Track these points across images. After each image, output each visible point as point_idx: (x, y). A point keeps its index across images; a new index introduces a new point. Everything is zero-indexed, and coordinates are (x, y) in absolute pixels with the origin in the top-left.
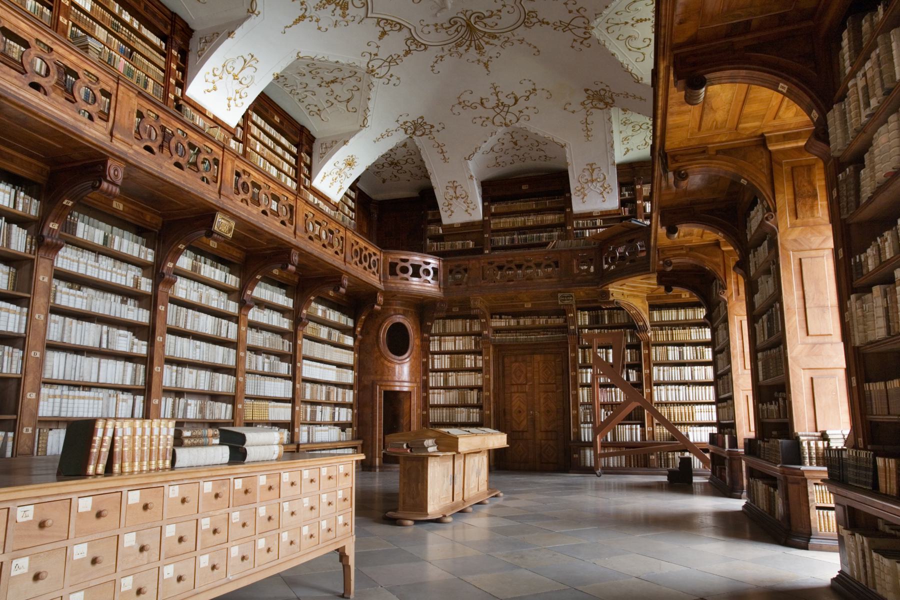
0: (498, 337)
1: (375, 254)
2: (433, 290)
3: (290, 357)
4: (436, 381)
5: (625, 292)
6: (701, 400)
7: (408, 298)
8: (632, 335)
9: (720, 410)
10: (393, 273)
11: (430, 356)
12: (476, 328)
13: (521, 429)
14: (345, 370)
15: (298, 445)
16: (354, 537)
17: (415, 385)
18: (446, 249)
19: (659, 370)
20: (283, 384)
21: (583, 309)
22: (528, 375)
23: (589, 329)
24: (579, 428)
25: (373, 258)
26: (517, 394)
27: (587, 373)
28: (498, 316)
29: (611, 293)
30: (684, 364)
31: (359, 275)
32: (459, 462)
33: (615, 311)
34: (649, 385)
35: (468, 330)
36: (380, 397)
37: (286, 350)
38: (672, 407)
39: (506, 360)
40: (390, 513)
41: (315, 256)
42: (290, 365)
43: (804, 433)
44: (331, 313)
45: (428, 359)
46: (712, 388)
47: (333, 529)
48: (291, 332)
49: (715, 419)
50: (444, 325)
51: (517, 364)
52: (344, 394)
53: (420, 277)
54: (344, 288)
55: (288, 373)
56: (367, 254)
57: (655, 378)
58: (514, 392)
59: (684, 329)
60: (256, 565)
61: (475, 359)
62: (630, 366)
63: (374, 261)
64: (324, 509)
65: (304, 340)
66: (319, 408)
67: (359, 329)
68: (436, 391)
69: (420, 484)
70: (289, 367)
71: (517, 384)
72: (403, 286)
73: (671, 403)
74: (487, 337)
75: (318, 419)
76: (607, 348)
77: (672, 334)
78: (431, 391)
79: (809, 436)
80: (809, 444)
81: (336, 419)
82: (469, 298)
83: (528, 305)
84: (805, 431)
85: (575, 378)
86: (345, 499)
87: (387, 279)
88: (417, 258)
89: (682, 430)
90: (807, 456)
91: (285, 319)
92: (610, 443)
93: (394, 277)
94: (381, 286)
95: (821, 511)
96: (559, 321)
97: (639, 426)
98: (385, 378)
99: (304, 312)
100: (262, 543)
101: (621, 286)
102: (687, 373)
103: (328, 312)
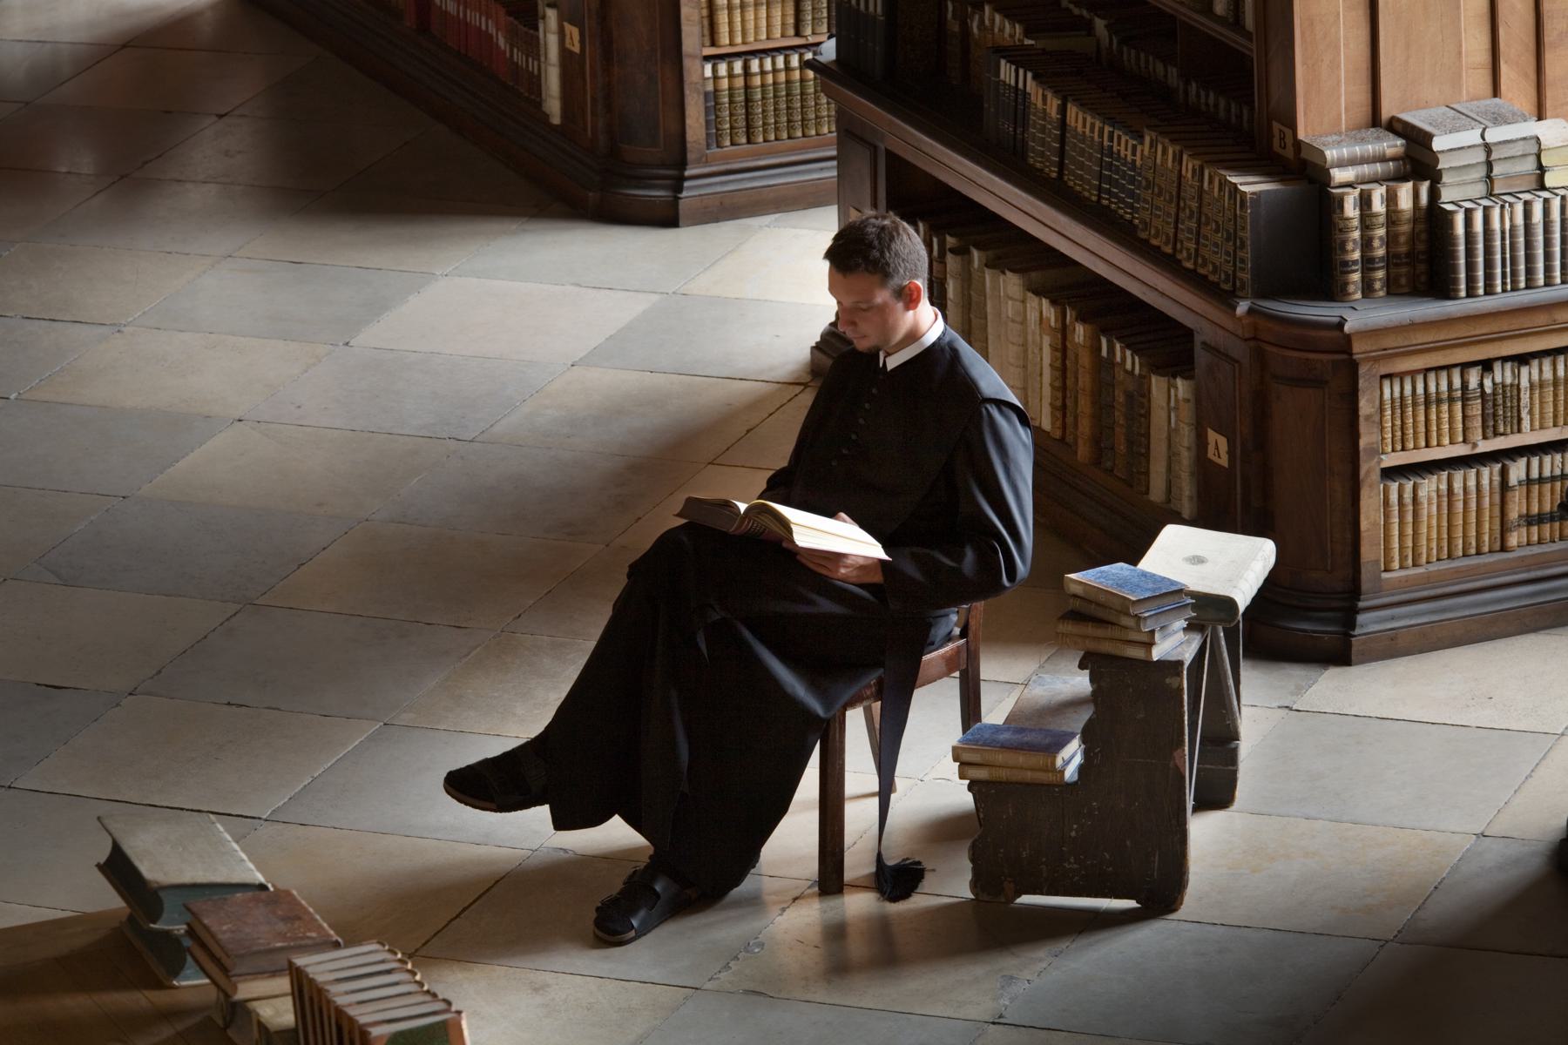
80: (1365, 201)
95: (1394, 486)
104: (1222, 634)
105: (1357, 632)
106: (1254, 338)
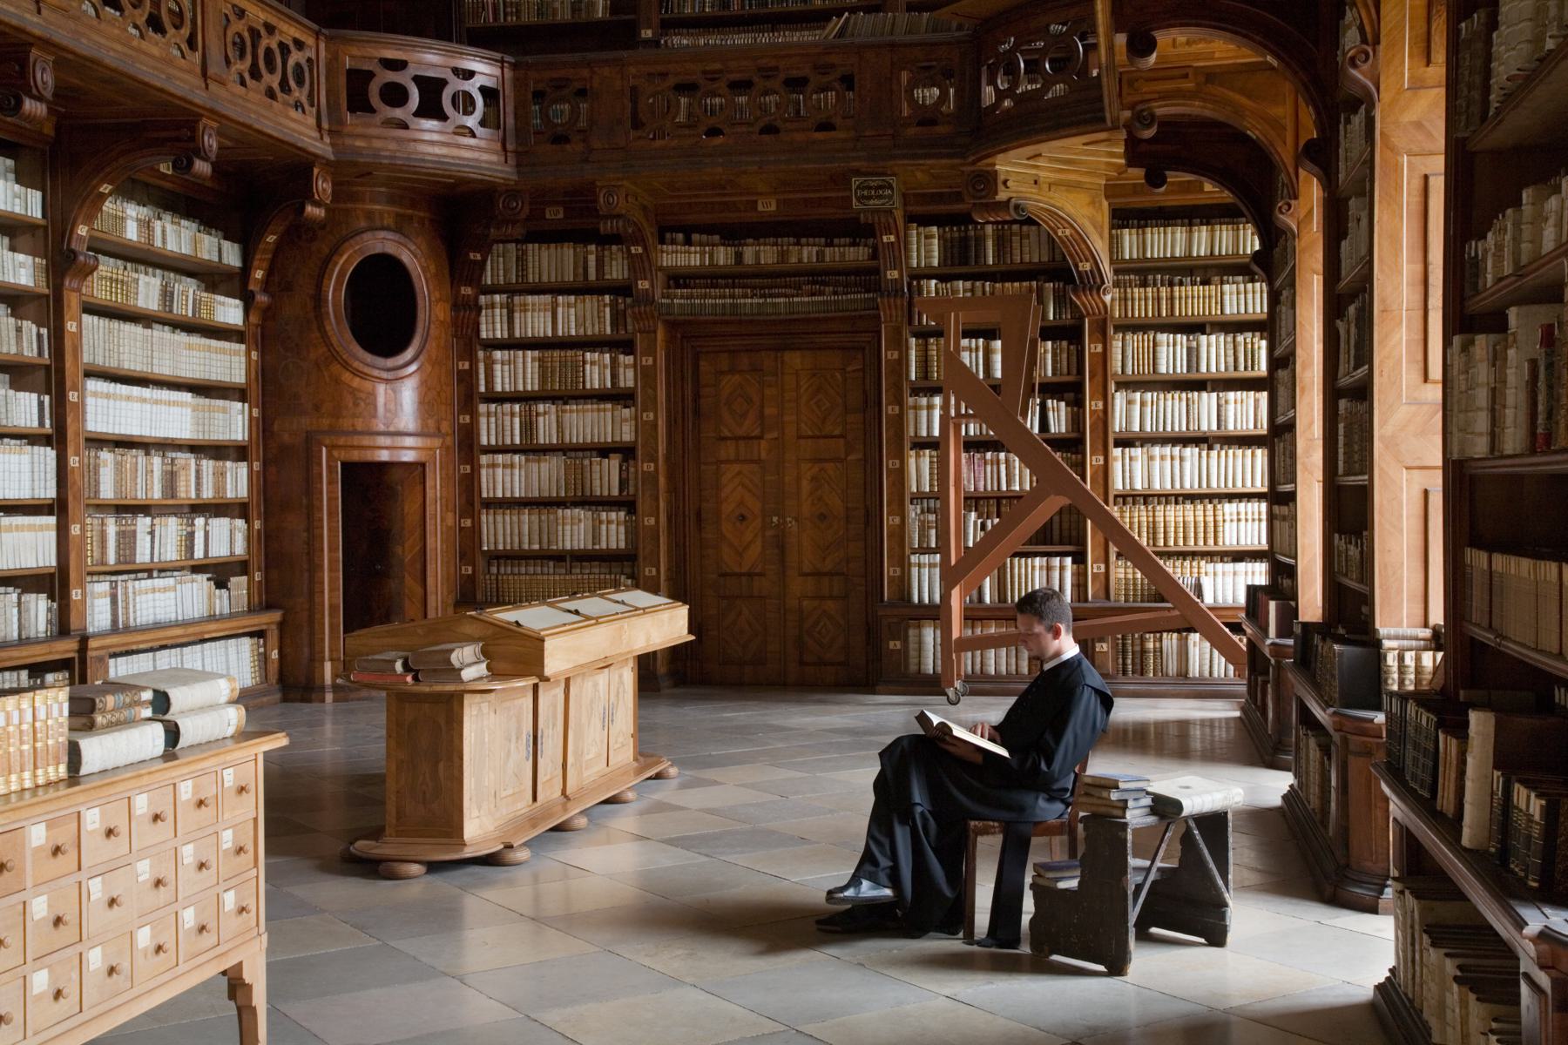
0: (680, 300)
1: (299, 45)
2: (485, 157)
3: (41, 374)
4: (500, 430)
5: (1042, 174)
6: (1239, 489)
7: (406, 180)
8: (1061, 300)
9: (1277, 523)
10: (359, 103)
11: (481, 354)
12: (617, 271)
13: (745, 570)
14: (220, 403)
15: (84, 640)
16: (265, 937)
17: (437, 442)
18: (525, 19)
19: (1130, 402)
20: (26, 458)
21: (924, 221)
22: (767, 411)
23: (943, 278)
24: (903, 563)
25: (295, 57)
26: (736, 468)
27: (930, 407)
28: (680, 236)
29: (1002, 177)
30: (1200, 385)
31: (252, 119)
32: (551, 698)
33: (1015, 227)
34: (1101, 447)
35: (592, 276)
36: (331, 482)
37: (30, 351)
38: (1160, 508)
39: (704, 365)
40: (360, 844)
41: (107, 67)
42: (47, 399)
43: (1392, 631)
44: (169, 227)
45: (474, 361)
46: (1261, 455)
47: (212, 925)
48: (39, 297)
49: (1264, 545)
50: (521, 260)
51: (737, 378)
52: (220, 475)
53: (442, 117)
54: (206, 159)
55: (41, 423)
56: (274, 46)
57: (1118, 424)
58: (728, 461)
59: (1205, 282)
60: (29, 1033)
61: (614, 361)
62: (1051, 390)
63: (298, 66)
64: (190, 882)
65: (87, 318)
66: (143, 523)
67: (259, 274)
68: (500, 458)
69: (441, 765)
70: (41, 404)
71: (737, 439)
72: (392, 146)
73: (1159, 496)
74: (648, 299)
75: (143, 556)
76: (989, 335)
77: (1172, 298)
78: (484, 459)
79: (1404, 638)
80: (1401, 659)
81: (199, 553)
82: (593, 183)
83: (768, 206)
84: (1400, 624)
85: (899, 422)
86: (240, 850)
87: (341, 122)
88: (431, 58)
89: (1181, 573)
91: (21, 257)
92: (988, 609)
93: (366, 117)
94: (321, 147)
96: (857, 254)
97: (1069, 560)
98: (345, 423)
99: (82, 230)
100: (41, 981)
101: (1028, 159)
102: (1206, 410)
103: (158, 225)
104: (1196, 832)
105: (1384, 896)
106: (1340, 730)
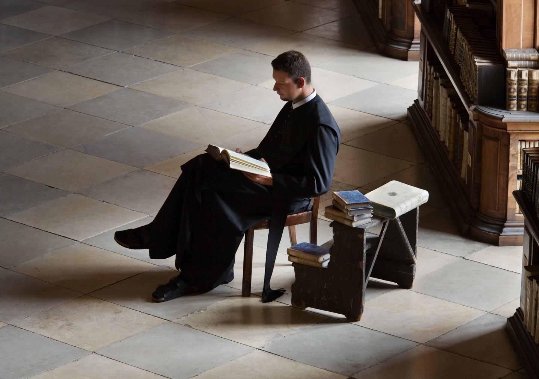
80: (520, 74)
90: (515, 94)
104: (400, 223)
105: (503, 234)
